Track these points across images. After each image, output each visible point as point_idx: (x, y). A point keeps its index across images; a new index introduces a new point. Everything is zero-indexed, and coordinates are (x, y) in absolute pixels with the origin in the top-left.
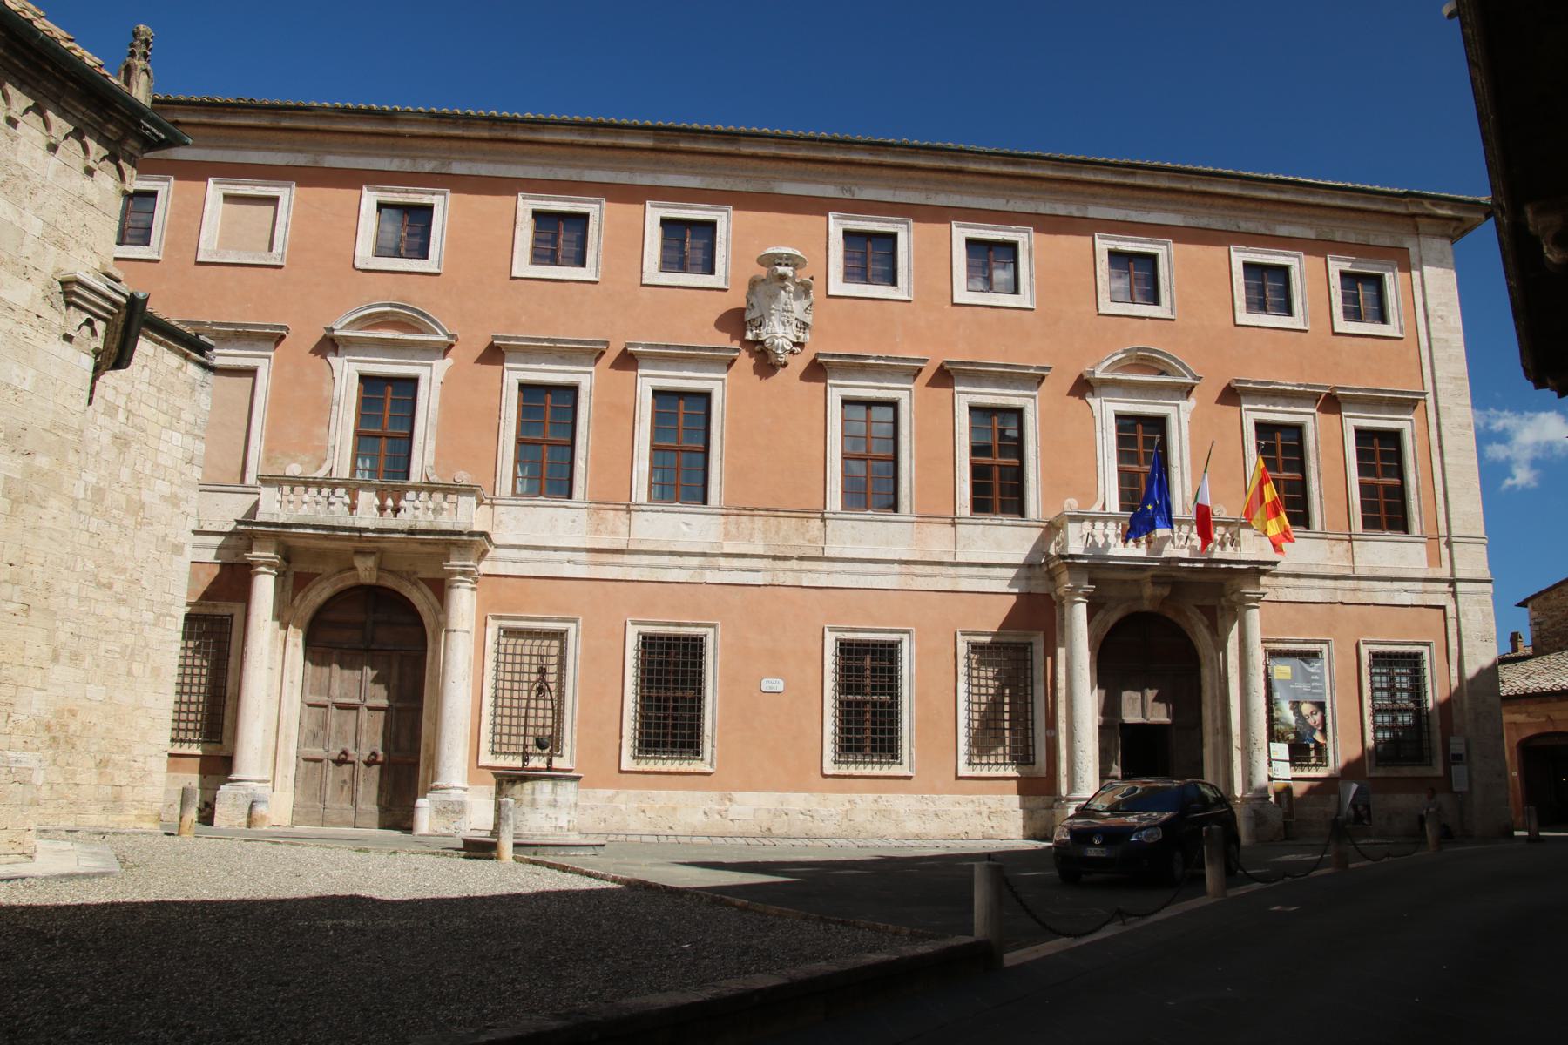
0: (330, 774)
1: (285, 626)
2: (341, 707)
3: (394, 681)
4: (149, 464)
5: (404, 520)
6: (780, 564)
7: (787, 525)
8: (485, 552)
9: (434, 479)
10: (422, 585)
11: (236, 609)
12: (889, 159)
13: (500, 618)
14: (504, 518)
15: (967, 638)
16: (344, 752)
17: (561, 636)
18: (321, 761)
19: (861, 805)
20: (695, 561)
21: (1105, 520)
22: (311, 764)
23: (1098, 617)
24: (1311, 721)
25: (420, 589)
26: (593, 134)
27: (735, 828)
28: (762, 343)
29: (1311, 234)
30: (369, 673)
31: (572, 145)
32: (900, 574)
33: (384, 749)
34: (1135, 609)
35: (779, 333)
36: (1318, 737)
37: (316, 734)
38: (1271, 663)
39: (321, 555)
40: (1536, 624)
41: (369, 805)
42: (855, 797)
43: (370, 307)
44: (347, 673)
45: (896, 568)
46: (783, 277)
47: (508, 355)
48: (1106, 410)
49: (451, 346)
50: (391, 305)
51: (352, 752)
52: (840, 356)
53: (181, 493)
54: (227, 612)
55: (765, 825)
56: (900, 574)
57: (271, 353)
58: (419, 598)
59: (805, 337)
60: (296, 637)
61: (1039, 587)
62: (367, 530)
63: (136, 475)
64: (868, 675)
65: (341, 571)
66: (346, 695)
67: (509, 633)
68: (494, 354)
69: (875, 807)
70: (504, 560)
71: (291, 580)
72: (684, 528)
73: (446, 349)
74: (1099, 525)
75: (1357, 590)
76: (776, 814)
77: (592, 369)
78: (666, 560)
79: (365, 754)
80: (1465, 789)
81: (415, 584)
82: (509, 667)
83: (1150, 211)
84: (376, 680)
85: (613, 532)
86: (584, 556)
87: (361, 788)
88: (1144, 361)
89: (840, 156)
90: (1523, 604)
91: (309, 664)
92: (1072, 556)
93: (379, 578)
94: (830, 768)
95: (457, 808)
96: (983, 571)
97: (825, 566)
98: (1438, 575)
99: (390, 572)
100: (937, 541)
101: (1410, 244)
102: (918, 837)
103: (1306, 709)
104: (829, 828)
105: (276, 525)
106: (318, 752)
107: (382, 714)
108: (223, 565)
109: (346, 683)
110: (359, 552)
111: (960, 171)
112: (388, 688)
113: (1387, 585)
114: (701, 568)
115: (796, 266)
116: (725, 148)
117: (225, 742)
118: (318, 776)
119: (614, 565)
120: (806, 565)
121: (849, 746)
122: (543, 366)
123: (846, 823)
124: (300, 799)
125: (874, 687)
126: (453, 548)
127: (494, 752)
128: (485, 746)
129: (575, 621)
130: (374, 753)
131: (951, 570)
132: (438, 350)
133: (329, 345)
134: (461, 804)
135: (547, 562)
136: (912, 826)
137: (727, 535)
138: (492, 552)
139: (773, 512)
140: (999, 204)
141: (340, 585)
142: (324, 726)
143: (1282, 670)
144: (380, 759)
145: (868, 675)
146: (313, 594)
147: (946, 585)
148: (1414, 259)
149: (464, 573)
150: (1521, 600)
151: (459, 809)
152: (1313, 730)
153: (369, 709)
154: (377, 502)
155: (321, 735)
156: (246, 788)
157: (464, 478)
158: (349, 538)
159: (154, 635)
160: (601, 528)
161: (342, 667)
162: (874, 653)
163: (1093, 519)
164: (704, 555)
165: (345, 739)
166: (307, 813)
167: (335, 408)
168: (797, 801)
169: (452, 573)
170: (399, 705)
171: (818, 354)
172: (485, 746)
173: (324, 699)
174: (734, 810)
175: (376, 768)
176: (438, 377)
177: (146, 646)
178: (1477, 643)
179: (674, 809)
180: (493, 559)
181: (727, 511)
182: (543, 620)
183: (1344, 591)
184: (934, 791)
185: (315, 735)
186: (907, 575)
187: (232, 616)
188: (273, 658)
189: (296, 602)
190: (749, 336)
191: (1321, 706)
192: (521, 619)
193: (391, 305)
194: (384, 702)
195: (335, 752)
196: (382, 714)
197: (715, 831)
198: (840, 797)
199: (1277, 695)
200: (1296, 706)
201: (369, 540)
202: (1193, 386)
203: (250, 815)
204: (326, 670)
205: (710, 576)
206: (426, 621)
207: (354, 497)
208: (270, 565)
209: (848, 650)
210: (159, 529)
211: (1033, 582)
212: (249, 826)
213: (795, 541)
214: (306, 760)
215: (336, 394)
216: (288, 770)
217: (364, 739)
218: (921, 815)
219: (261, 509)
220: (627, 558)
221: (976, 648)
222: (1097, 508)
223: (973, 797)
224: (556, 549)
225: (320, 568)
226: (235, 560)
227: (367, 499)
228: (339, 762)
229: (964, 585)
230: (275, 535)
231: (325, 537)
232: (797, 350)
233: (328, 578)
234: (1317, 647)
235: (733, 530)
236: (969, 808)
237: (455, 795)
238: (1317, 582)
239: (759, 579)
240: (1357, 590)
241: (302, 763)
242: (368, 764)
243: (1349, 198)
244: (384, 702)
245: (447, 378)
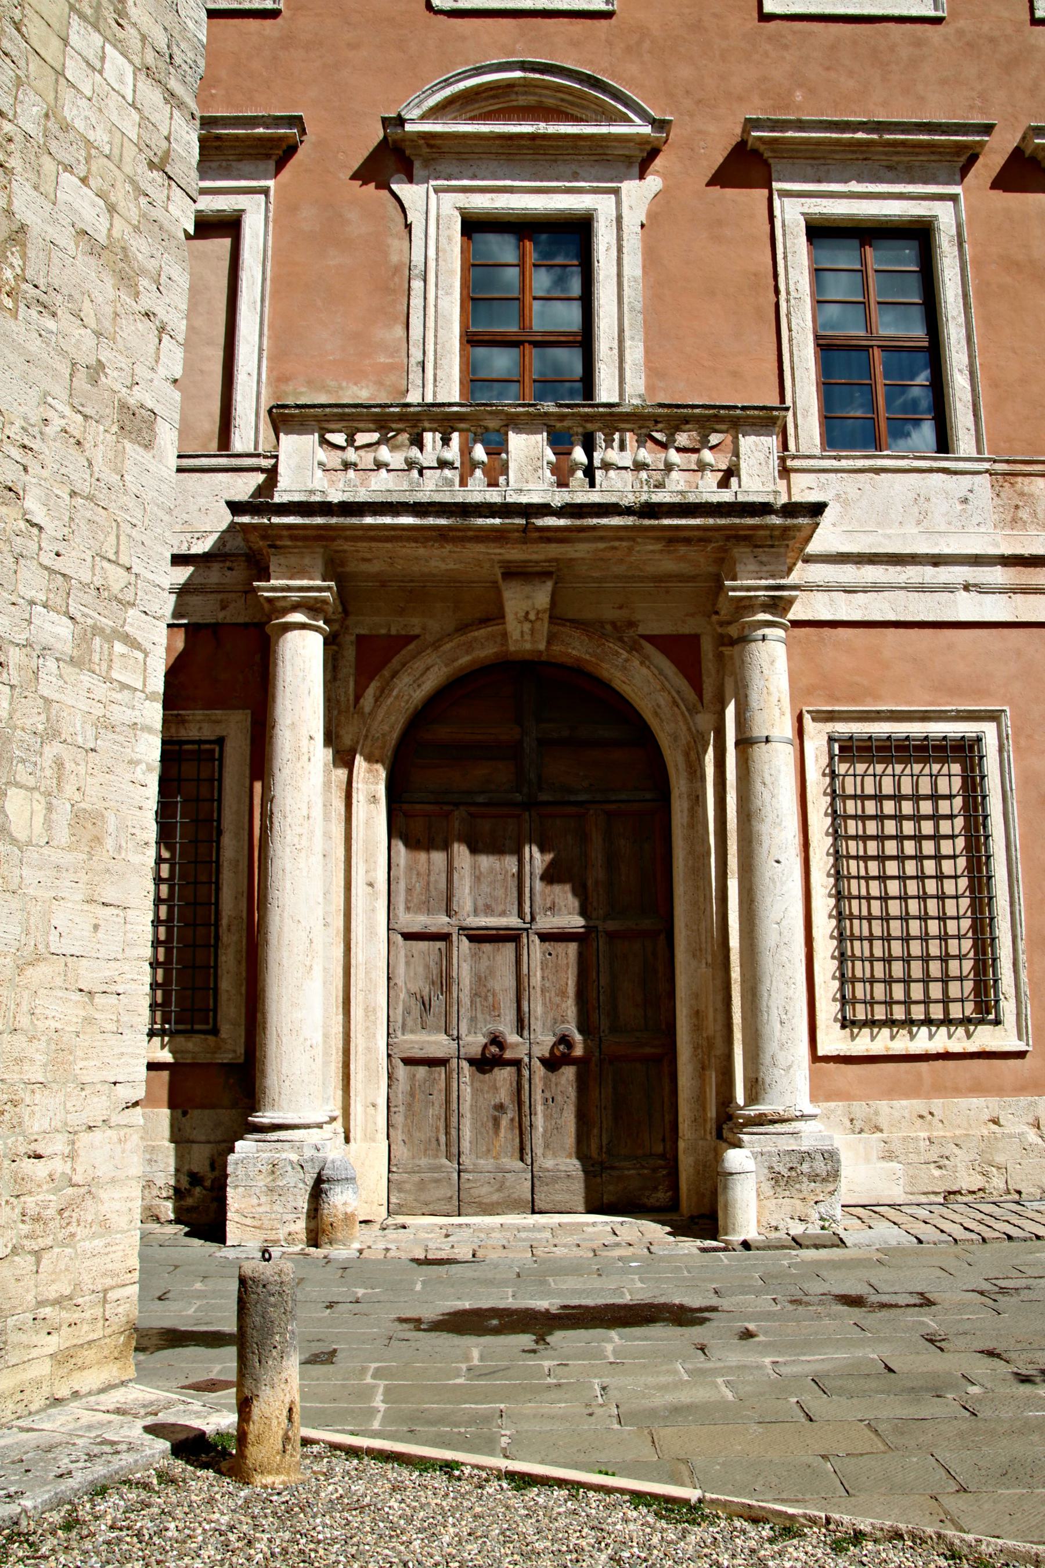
0: (467, 1091)
1: (344, 759)
2: (479, 937)
3: (597, 873)
5: (618, 486)
10: (649, 648)
11: (234, 727)
13: (831, 717)
16: (496, 1040)
17: (965, 752)
18: (442, 1062)
22: (422, 1071)
25: (645, 660)
30: (537, 859)
33: (581, 1031)
37: (430, 1000)
39: (416, 593)
41: (562, 1163)
43: (479, 71)
44: (486, 861)
47: (776, 166)
49: (654, 153)
50: (523, 66)
51: (513, 1038)
54: (208, 732)
57: (270, 183)
58: (644, 683)
60: (371, 781)
65: (463, 628)
66: (488, 910)
67: (850, 750)
68: (747, 165)
71: (350, 653)
73: (642, 158)
77: (956, 189)
79: (544, 1042)
81: (634, 647)
84: (550, 877)
87: (539, 1121)
91: (399, 846)
93: (551, 639)
95: (821, 1167)
99: (577, 623)
105: (326, 508)
106: (437, 1044)
107: (573, 947)
108: (192, 631)
109: (479, 884)
112: (581, 892)
117: (226, 1030)
118: (439, 1097)
122: (854, 186)
124: (401, 1152)
126: (740, 551)
127: (846, 1023)
129: (993, 716)
130: (564, 1040)
132: (628, 160)
133: (394, 158)
134: (831, 1156)
141: (464, 660)
142: (445, 981)
144: (578, 1051)
146: (404, 681)
151: (824, 1170)
153: (544, 937)
155: (438, 1004)
156: (298, 1146)
159: (76, 696)
160: (1024, 514)
161: (474, 850)
165: (494, 1009)
166: (422, 1185)
167: (417, 285)
170: (612, 926)
172: (827, 1009)
173: (439, 922)
175: (569, 1073)
176: (634, 217)
177: (52, 734)
182: (925, 717)
185: (426, 1006)
187: (221, 741)
188: (324, 829)
189: (368, 701)
193: (523, 66)
194: (576, 922)
195: (475, 1042)
196: (573, 947)
201: (549, 535)
203: (315, 1212)
204: (438, 858)
207: (497, 449)
208: (312, 608)
210: (83, 344)
212: (314, 1238)
214: (408, 1061)
215: (417, 258)
216: (371, 1090)
217: (537, 1008)
219: (284, 481)
224: (937, 560)
225: (414, 624)
226: (221, 617)
227: (526, 448)
228: (483, 1064)
230: (322, 534)
231: (442, 535)
233: (436, 645)
237: (811, 1135)
241: (401, 1071)
242: (552, 1064)
244: (576, 922)
245: (652, 215)
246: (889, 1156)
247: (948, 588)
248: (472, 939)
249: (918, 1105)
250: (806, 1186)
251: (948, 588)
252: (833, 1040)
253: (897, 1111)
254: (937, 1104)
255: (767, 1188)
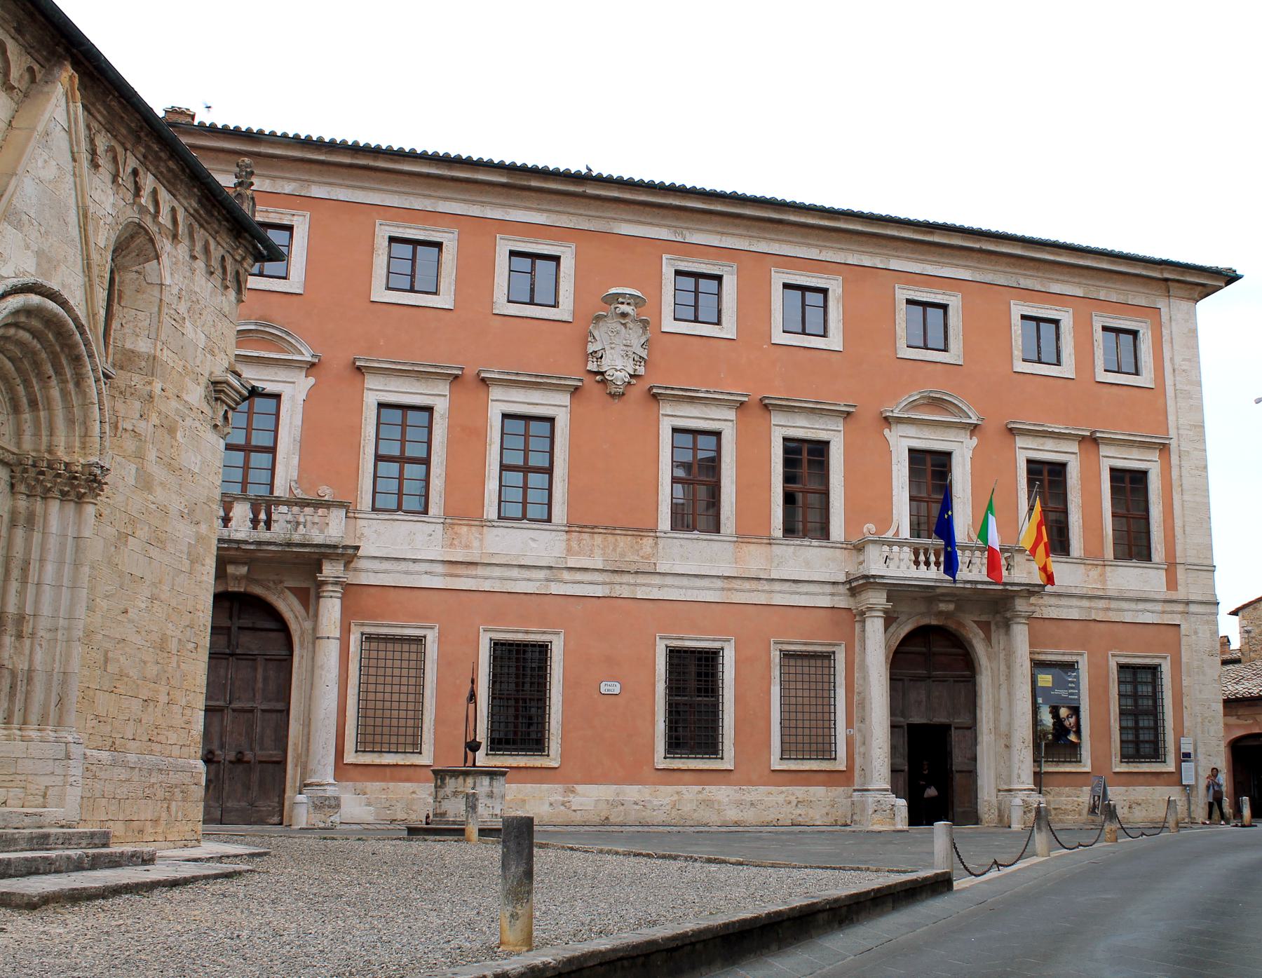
5: (279, 530)
6: (617, 578)
7: (623, 542)
9: (299, 493)
10: (288, 593)
12: (719, 208)
14: (366, 531)
15: (779, 646)
19: (687, 796)
20: (541, 574)
21: (901, 544)
23: (892, 629)
24: (1067, 723)
26: (450, 168)
27: (578, 818)
28: (602, 373)
29: (1079, 292)
31: (428, 176)
32: (723, 589)
34: (925, 621)
35: (618, 366)
36: (1072, 737)
38: (1036, 671)
40: (1246, 632)
42: (682, 788)
45: (719, 584)
46: (624, 315)
48: (901, 442)
52: (672, 389)
55: (604, 815)
56: (723, 589)
58: (288, 607)
59: (641, 370)
61: (843, 602)
64: (694, 675)
69: (700, 797)
72: (533, 544)
74: (895, 548)
75: (1108, 609)
76: (612, 804)
78: (515, 573)
80: (1192, 782)
82: (372, 671)
83: (944, 264)
85: (467, 547)
88: (936, 403)
89: (677, 202)
90: (1235, 613)
92: (874, 576)
94: (661, 762)
95: (333, 803)
96: (794, 587)
97: (657, 580)
98: (1174, 598)
100: (755, 559)
101: (1161, 303)
102: (737, 824)
103: (1063, 712)
104: (660, 817)
111: (780, 222)
113: (1133, 606)
114: (548, 580)
115: (636, 305)
116: (572, 188)
120: (641, 579)
121: (675, 745)
123: (674, 813)
125: (699, 690)
128: (350, 744)
129: (432, 628)
131: (767, 587)
134: (337, 799)
136: (732, 814)
137: (569, 550)
139: (611, 530)
140: (813, 253)
143: (1045, 680)
145: (694, 675)
147: (762, 599)
148: (1165, 318)
150: (1233, 609)
152: (1067, 731)
157: (327, 493)
162: (700, 659)
163: (890, 544)
164: (551, 568)
168: (632, 792)
171: (651, 388)
172: (350, 744)
174: (576, 802)
178: (1205, 657)
179: (524, 801)
181: (570, 528)
183: (1097, 611)
184: (751, 783)
186: (729, 589)
190: (592, 366)
191: (1076, 711)
192: (383, 626)
197: (560, 820)
198: (670, 789)
199: (1040, 700)
200: (1055, 711)
202: (976, 425)
205: (555, 589)
206: (294, 627)
209: (677, 657)
211: (836, 598)
213: (631, 557)
218: (739, 804)
221: (786, 655)
222: (889, 534)
223: (784, 788)
229: (778, 600)
232: (633, 381)
234: (1074, 658)
235: (574, 545)
236: (781, 799)
237: (330, 791)
238: (1074, 602)
239: (599, 591)
240: (1108, 609)
243: (1113, 263)
246: (369, 804)
247: (418, 573)
249: (383, 785)
250: (327, 809)
251: (418, 573)
252: (350, 757)
253: (374, 787)
254: (391, 785)
255: (311, 810)
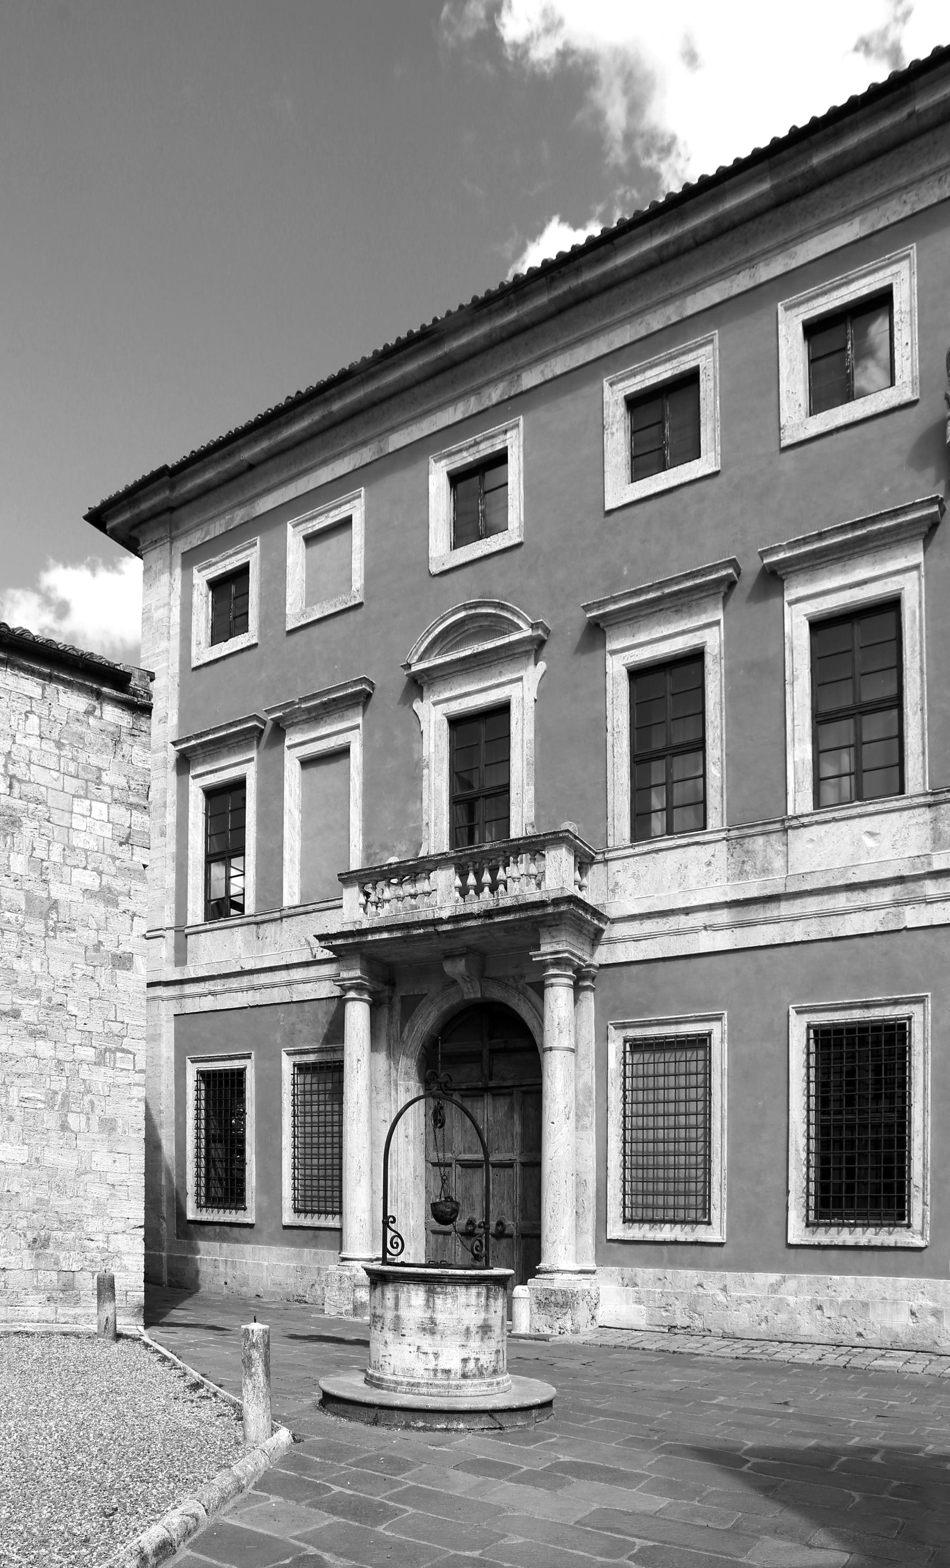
2: (467, 1165)
4: (57, 849)
8: (600, 931)
53: (118, 884)
62: (440, 921)
63: (39, 866)
66: (470, 1150)
70: (624, 940)
86: (723, 916)
110: (450, 956)
119: (766, 922)
135: (678, 933)
138: (612, 931)
149: (558, 963)
154: (458, 882)
158: (426, 936)
169: (544, 966)
180: (611, 941)
220: (786, 909)
248: (462, 1166)
